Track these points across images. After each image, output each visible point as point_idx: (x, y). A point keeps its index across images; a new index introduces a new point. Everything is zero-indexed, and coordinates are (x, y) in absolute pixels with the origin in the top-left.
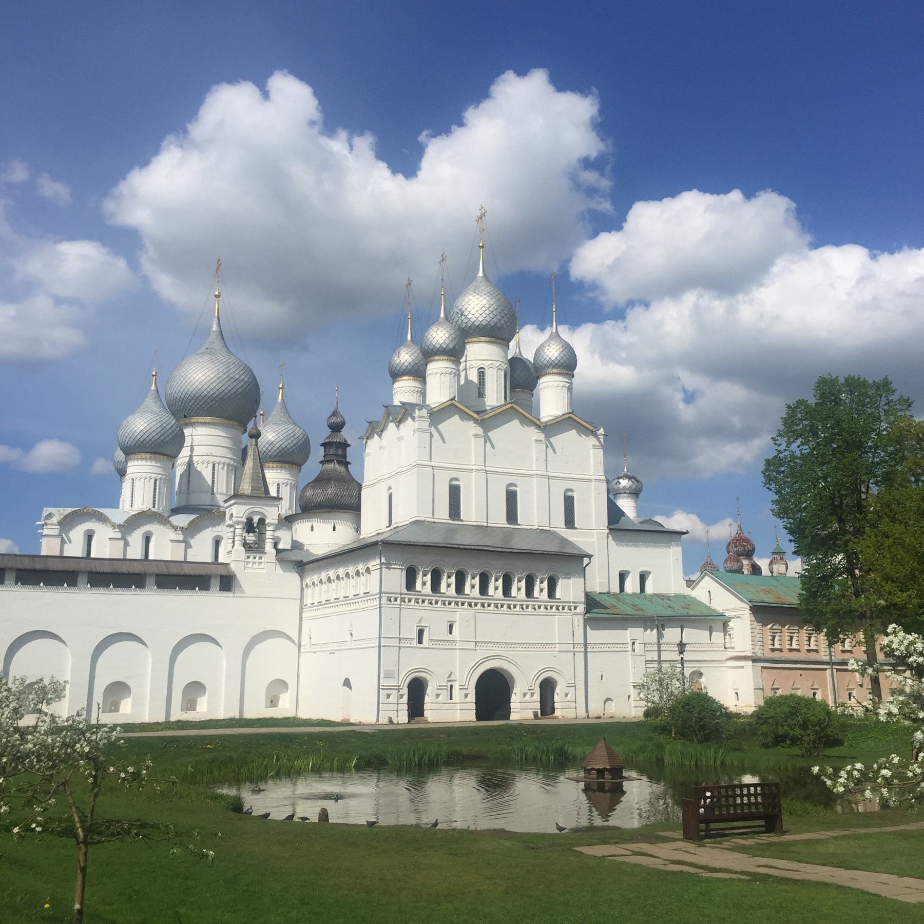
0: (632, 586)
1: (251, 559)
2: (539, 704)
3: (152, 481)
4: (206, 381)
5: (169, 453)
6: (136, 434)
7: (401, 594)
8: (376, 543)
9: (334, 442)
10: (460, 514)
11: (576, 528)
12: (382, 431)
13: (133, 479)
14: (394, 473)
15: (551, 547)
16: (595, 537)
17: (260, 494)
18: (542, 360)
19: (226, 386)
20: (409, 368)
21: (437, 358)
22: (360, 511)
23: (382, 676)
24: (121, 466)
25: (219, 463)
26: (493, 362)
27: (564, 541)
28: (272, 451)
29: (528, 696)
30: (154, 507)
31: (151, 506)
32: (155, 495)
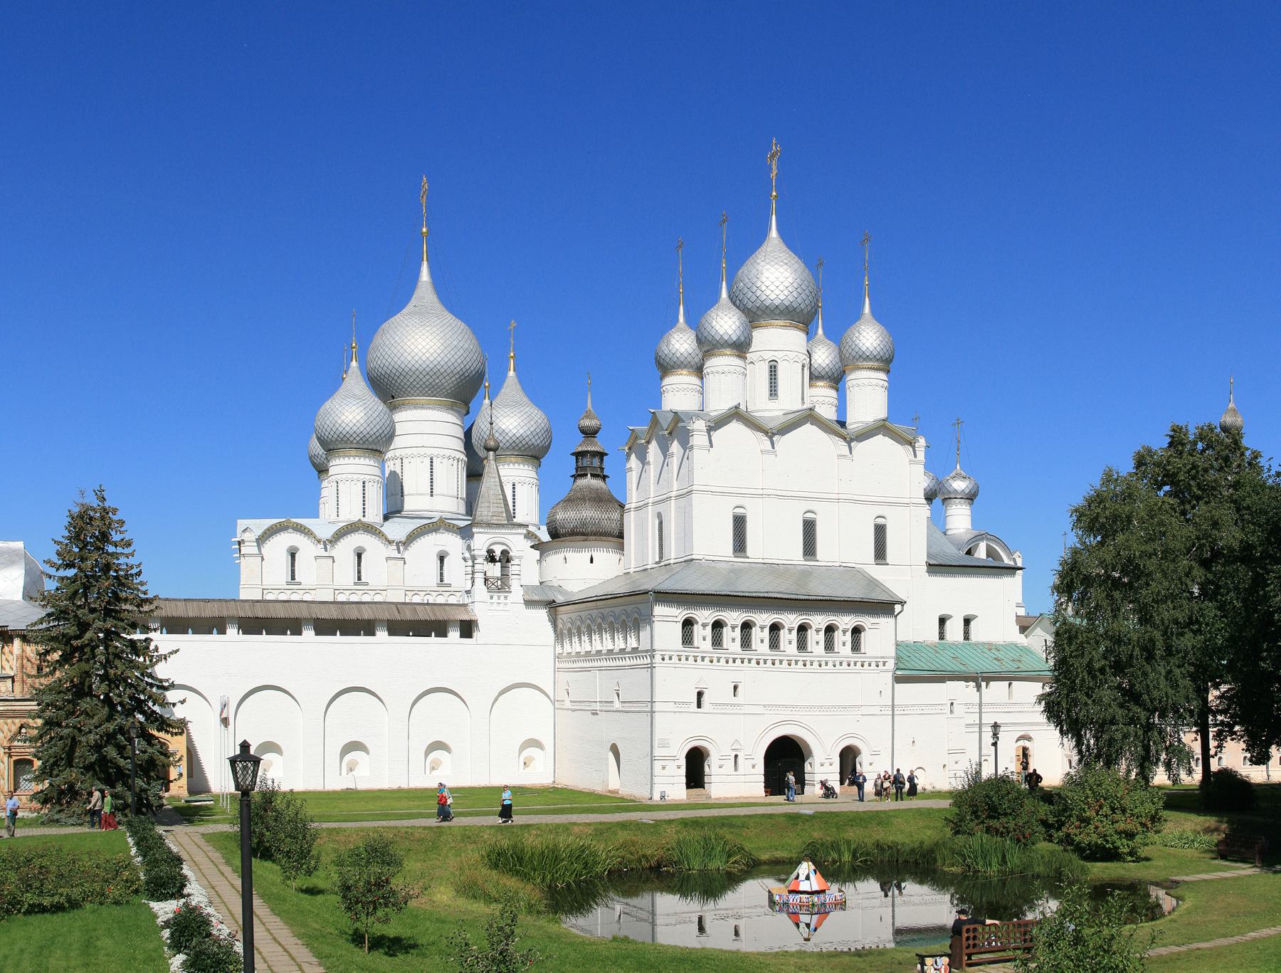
0: (954, 631)
17: (501, 520)
23: (656, 744)
27: (873, 583)
29: (827, 765)
30: (364, 516)
31: (360, 516)
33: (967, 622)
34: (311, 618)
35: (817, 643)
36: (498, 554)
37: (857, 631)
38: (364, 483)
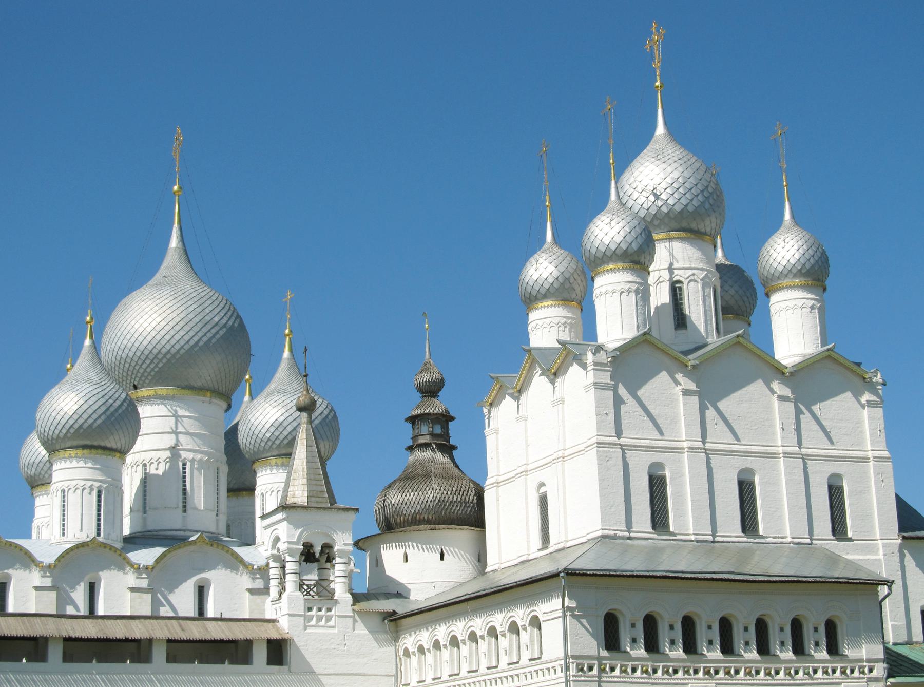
1: (314, 612)
3: (95, 493)
4: (168, 328)
5: (119, 447)
6: (67, 417)
7: (599, 659)
8: (555, 575)
9: (429, 414)
10: (668, 524)
11: (850, 540)
12: (520, 392)
13: (64, 491)
14: (550, 459)
15: (813, 569)
16: (881, 552)
18: (775, 265)
19: (200, 334)
20: (556, 285)
21: (612, 266)
22: (484, 528)
24: (34, 470)
25: (192, 461)
26: (695, 272)
28: (281, 437)
30: (99, 535)
32: (99, 515)
34: (60, 637)
36: (317, 549)
37: (831, 628)
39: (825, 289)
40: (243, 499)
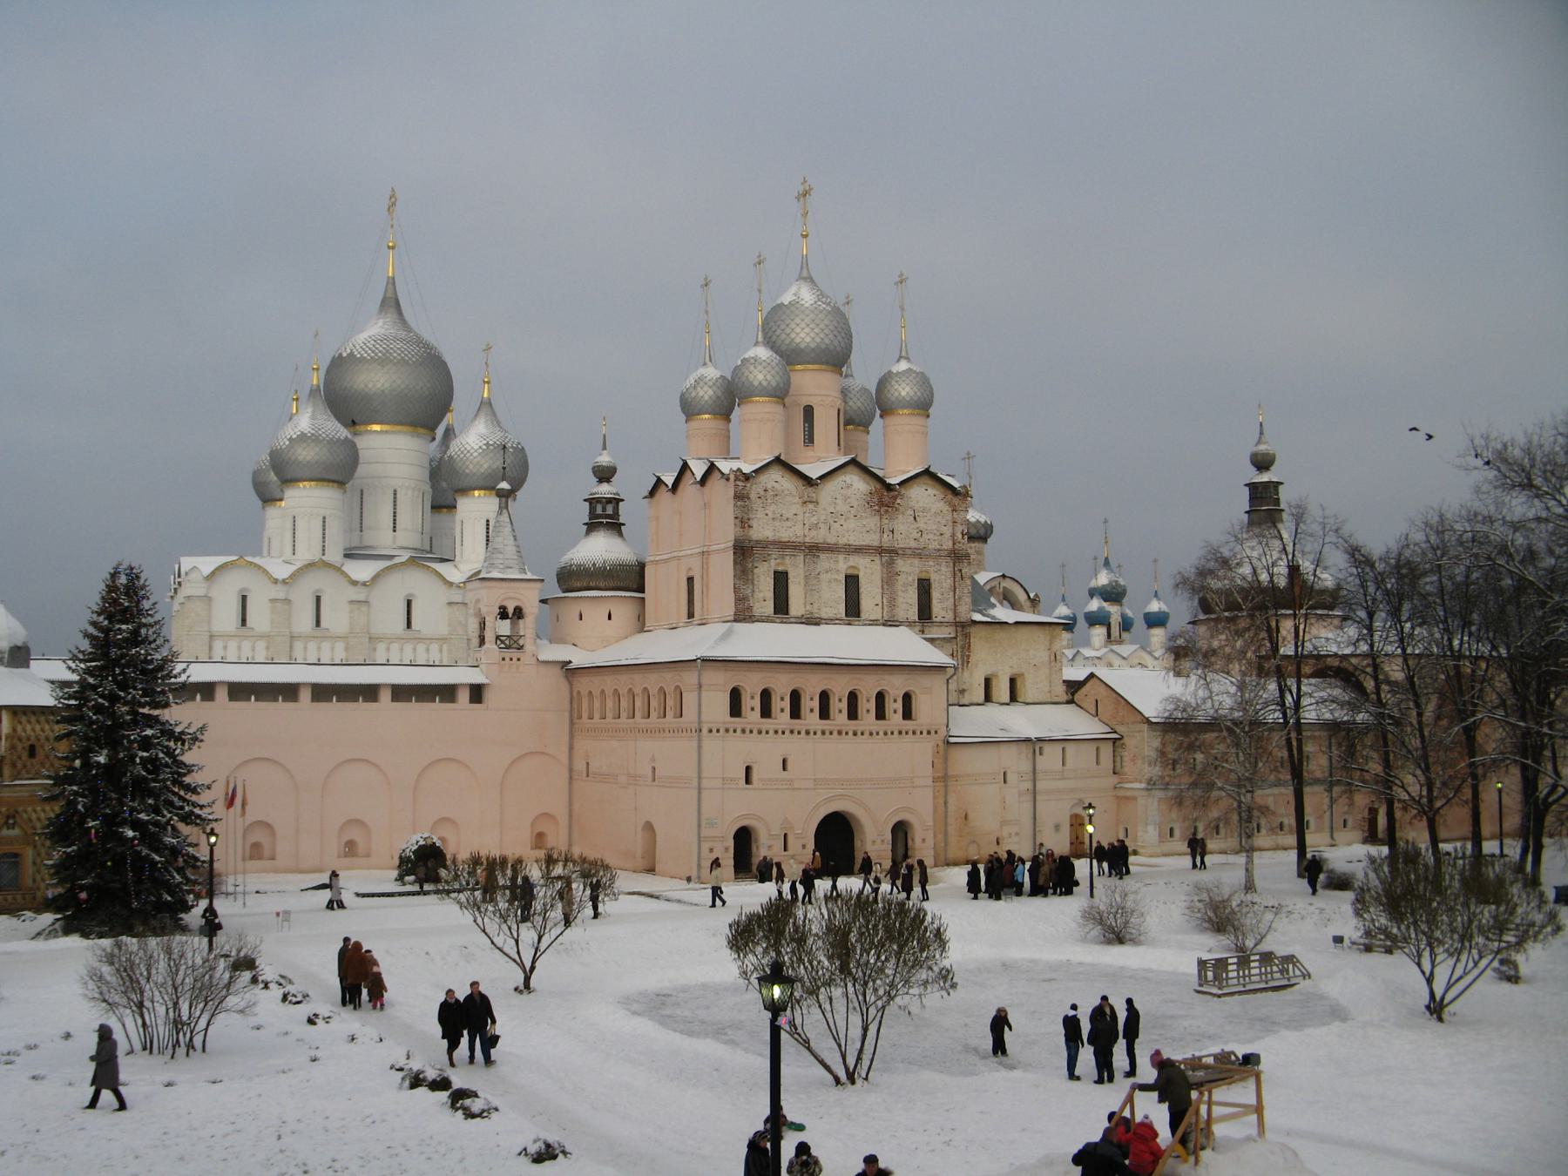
2: (890, 853)
7: (724, 723)
26: (824, 398)
30: (324, 554)
33: (1013, 681)
35: (868, 711)
36: (511, 611)
37: (907, 698)
38: (324, 518)
39: (928, 416)
40: (444, 516)
